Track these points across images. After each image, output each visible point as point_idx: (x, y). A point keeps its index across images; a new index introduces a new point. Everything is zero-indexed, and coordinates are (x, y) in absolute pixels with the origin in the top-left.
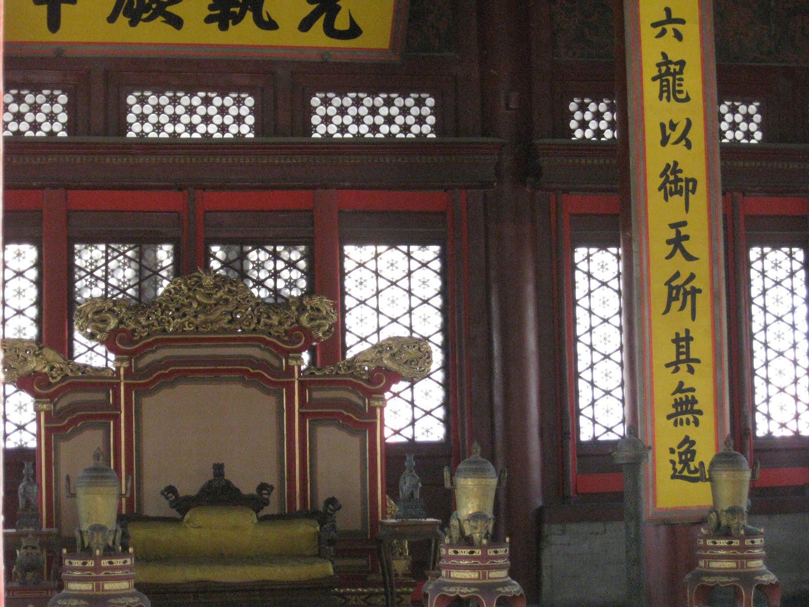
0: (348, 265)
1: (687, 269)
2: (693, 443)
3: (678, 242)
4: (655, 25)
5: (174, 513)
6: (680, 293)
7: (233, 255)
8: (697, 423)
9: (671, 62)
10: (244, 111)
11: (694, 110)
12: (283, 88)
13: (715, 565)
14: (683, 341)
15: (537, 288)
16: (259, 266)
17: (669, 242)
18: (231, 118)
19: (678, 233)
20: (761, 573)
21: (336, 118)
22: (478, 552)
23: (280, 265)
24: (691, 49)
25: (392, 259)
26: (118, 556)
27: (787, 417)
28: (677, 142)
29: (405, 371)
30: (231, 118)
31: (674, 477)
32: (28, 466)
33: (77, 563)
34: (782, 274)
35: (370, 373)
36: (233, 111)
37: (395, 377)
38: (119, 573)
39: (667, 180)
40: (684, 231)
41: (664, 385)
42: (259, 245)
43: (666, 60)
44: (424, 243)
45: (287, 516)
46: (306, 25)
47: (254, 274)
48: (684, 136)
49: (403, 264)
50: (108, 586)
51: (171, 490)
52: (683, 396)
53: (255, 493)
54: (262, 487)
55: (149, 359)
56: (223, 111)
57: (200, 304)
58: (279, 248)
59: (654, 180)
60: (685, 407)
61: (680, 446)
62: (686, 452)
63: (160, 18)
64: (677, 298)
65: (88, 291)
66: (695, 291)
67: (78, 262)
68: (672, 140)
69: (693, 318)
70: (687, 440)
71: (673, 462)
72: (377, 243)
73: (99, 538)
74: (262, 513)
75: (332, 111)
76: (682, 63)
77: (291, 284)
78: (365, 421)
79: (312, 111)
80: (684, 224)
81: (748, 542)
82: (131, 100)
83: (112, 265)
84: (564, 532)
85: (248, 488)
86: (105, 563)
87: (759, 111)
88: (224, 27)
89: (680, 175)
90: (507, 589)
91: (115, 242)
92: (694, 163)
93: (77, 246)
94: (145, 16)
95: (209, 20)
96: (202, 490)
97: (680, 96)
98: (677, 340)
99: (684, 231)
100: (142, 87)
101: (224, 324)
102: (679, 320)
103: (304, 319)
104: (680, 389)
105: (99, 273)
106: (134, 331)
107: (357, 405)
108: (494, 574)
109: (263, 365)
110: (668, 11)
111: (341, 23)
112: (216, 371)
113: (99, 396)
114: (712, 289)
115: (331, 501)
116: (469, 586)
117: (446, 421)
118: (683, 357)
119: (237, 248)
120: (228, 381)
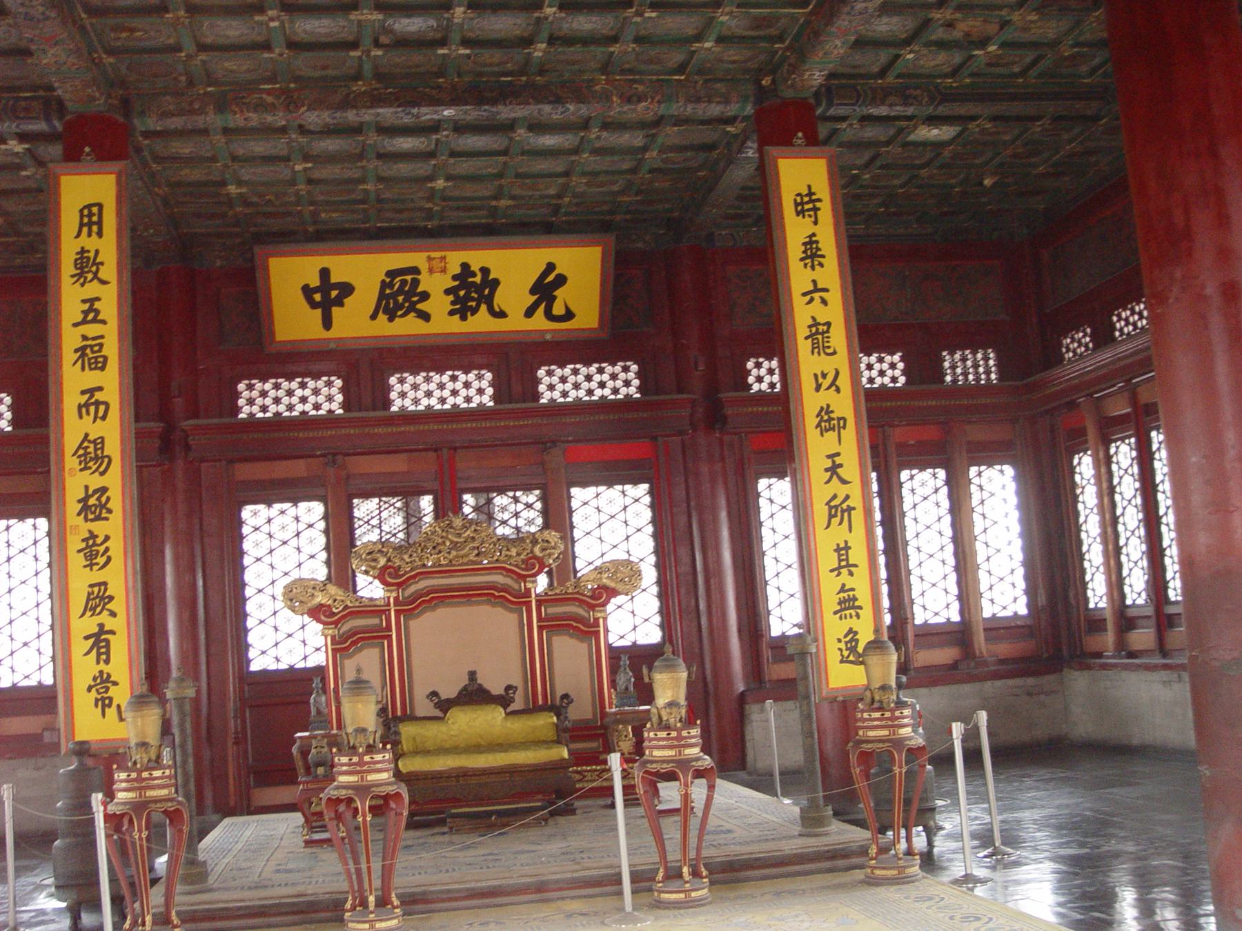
0: (575, 504)
1: (842, 491)
2: (856, 633)
3: (833, 470)
4: (804, 294)
5: (440, 714)
6: (839, 511)
7: (482, 501)
8: (858, 616)
10: (484, 384)
11: (841, 361)
12: (514, 362)
13: (871, 733)
14: (842, 550)
15: (729, 514)
16: (504, 509)
17: (827, 470)
18: (473, 390)
19: (834, 462)
20: (910, 738)
21: (559, 385)
22: (674, 734)
23: (520, 507)
24: (834, 311)
25: (611, 497)
26: (379, 752)
29: (619, 587)
30: (473, 390)
31: (842, 662)
32: (316, 682)
33: (344, 760)
34: (928, 490)
35: (593, 590)
36: (476, 384)
37: (614, 593)
38: (379, 766)
40: (838, 460)
42: (502, 491)
44: (635, 482)
45: (532, 709)
46: (529, 313)
47: (499, 516)
48: (833, 383)
49: (620, 501)
51: (434, 694)
52: (845, 595)
53: (502, 692)
54: (509, 688)
55: (412, 589)
56: (467, 385)
57: (452, 542)
58: (518, 494)
59: (811, 421)
60: (848, 604)
61: (845, 636)
62: (850, 641)
63: (413, 314)
64: (835, 516)
65: (366, 536)
66: (850, 509)
67: (357, 513)
68: (824, 387)
69: (850, 531)
70: (850, 631)
71: (840, 649)
72: (596, 483)
73: (361, 738)
74: (509, 709)
75: (555, 380)
76: (828, 324)
77: (530, 522)
78: (589, 630)
79: (538, 382)
80: (838, 454)
81: (897, 713)
83: (385, 515)
85: (497, 689)
86: (367, 758)
87: (902, 359)
88: (464, 318)
89: (832, 415)
90: (700, 763)
91: (386, 495)
92: (843, 405)
93: (356, 501)
94: (400, 313)
95: (451, 313)
96: (460, 693)
98: (838, 550)
99: (838, 460)
100: (401, 370)
101: (472, 557)
102: (838, 534)
103: (537, 550)
104: (843, 590)
105: (375, 522)
106: (399, 567)
107: (583, 618)
108: (688, 751)
109: (505, 589)
110: (814, 282)
111: (558, 309)
112: (467, 595)
113: (375, 621)
115: (565, 696)
116: (668, 762)
117: (662, 626)
118: (843, 563)
119: (485, 495)
120: (479, 603)
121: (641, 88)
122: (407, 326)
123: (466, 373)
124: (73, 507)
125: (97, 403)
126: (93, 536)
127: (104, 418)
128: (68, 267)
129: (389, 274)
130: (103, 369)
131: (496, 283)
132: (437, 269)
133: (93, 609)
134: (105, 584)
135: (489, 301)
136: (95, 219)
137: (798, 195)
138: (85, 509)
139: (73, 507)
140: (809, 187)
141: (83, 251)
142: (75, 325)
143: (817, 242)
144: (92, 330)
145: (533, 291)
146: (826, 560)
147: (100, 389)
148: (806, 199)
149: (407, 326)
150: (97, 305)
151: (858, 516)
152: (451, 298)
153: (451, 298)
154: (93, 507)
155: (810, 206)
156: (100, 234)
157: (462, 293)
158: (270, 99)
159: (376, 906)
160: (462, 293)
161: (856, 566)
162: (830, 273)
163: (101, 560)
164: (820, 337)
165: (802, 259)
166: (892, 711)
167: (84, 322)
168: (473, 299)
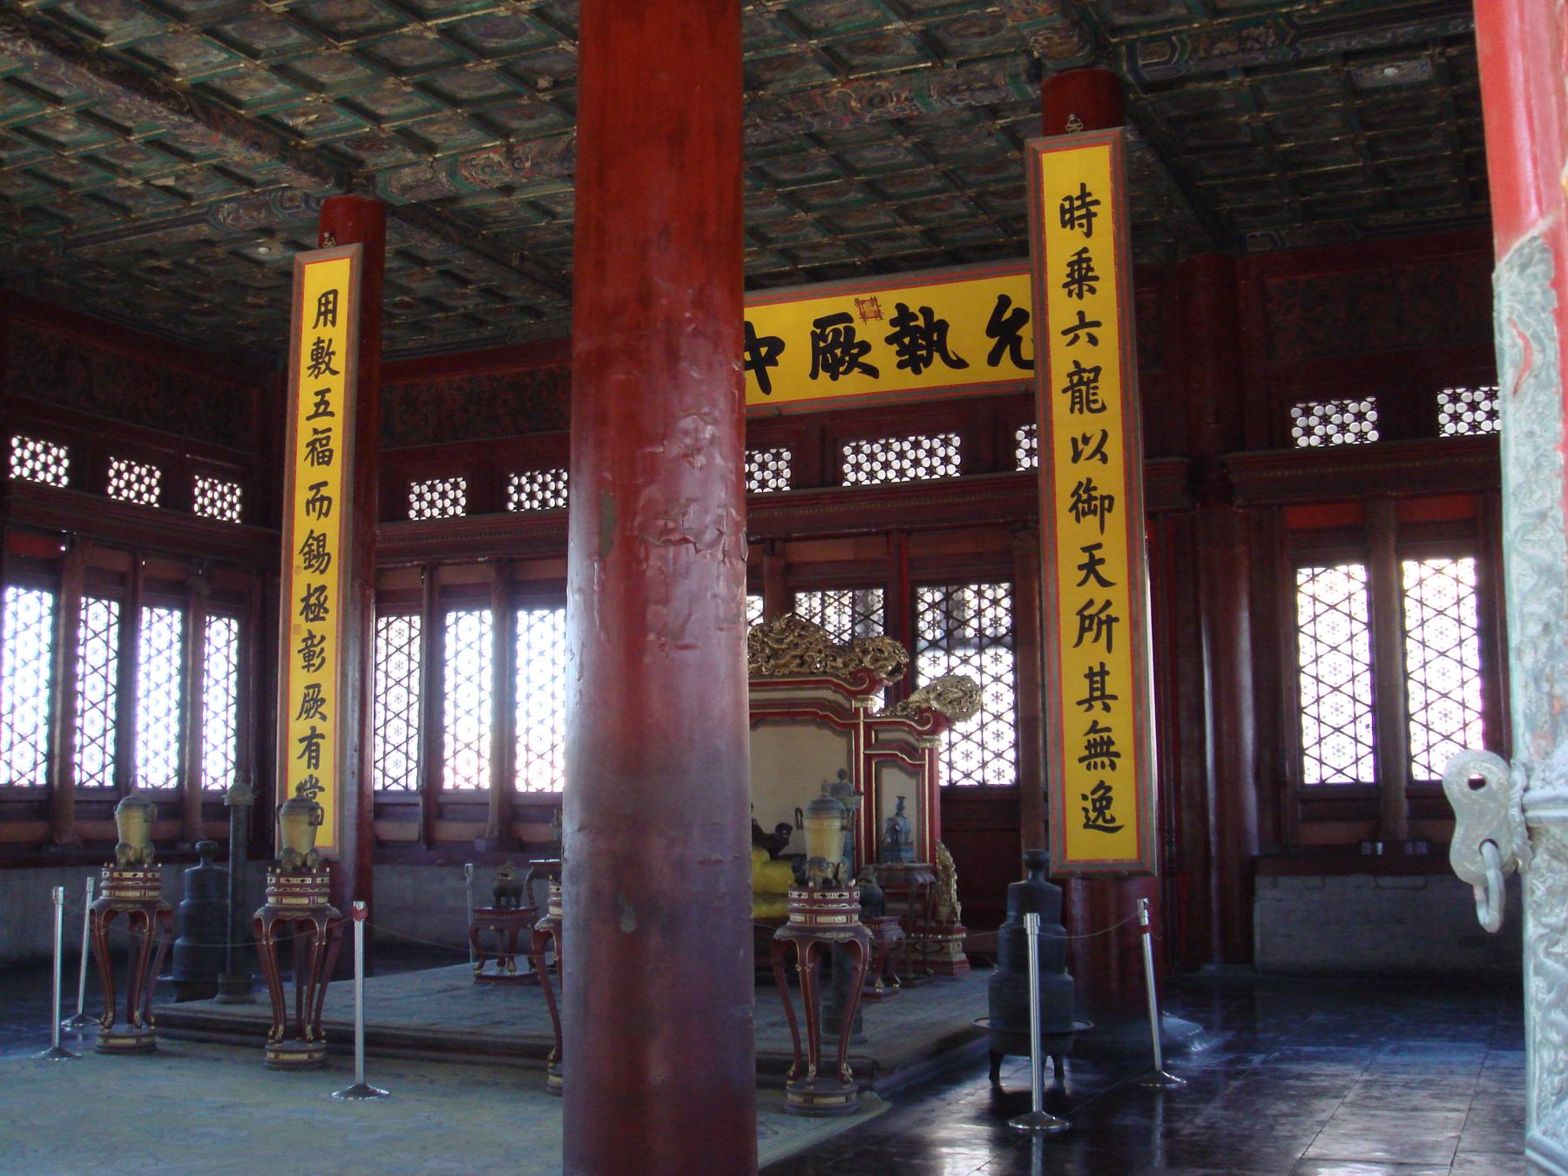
1: (1100, 595)
2: (1109, 789)
3: (1091, 567)
4: (1065, 333)
7: (938, 596)
8: (1113, 766)
9: (1085, 371)
14: (1096, 676)
17: (1081, 568)
18: (937, 458)
19: (1092, 556)
27: (972, 765)
28: (1091, 457)
29: (949, 712)
30: (937, 458)
31: (1086, 826)
39: (1079, 500)
40: (1098, 554)
41: (1074, 726)
43: (1079, 369)
46: (994, 359)
48: (1098, 450)
50: (823, 919)
52: (1097, 736)
58: (984, 587)
59: (1064, 501)
60: (1100, 748)
61: (1093, 792)
62: (1100, 799)
63: (856, 370)
64: (1090, 629)
66: (1111, 620)
69: (1109, 649)
70: (1101, 785)
76: (1097, 370)
78: (916, 761)
80: (1099, 546)
82: (847, 450)
84: (1275, 886)
89: (1094, 493)
94: (842, 369)
95: (901, 365)
97: (1094, 406)
98: (1090, 675)
99: (1098, 554)
101: (793, 666)
102: (1092, 653)
104: (1094, 728)
110: (1081, 314)
114: (1131, 616)
118: (1097, 694)
121: (884, 85)
122: (852, 384)
123: (931, 438)
124: (297, 606)
125: (323, 499)
126: (312, 636)
127: (326, 515)
128: (306, 360)
129: (820, 323)
130: (328, 463)
131: (943, 326)
132: (872, 311)
133: (308, 711)
134: (318, 686)
135: (941, 347)
136: (330, 307)
137: (1069, 198)
138: (307, 608)
139: (297, 606)
140: (1083, 186)
141: (320, 341)
142: (309, 418)
143: (1089, 259)
144: (322, 423)
145: (991, 332)
146: (1074, 687)
147: (325, 484)
148: (1077, 203)
149: (852, 384)
150: (328, 397)
151: (1121, 631)
152: (895, 347)
153: (895, 347)
154: (314, 610)
155: (1083, 212)
156: (334, 323)
157: (907, 340)
158: (496, 158)
159: (286, 1036)
160: (907, 340)
161: (1114, 697)
162: (1104, 302)
163: (317, 661)
164: (1084, 388)
165: (1066, 285)
166: (811, 891)
167: (316, 415)
168: (921, 347)
